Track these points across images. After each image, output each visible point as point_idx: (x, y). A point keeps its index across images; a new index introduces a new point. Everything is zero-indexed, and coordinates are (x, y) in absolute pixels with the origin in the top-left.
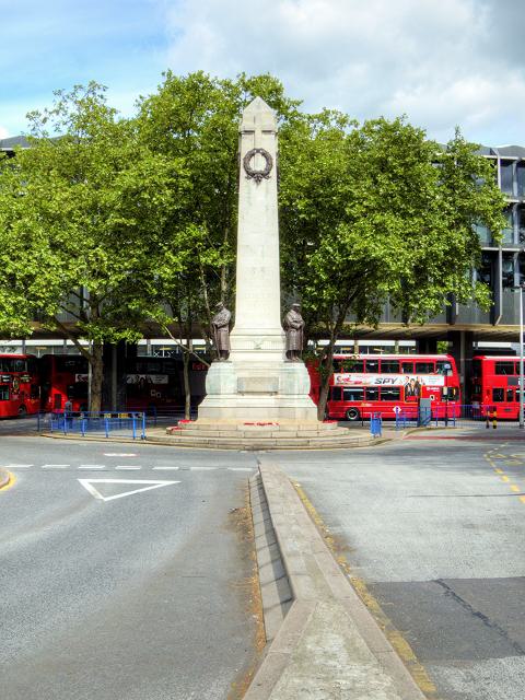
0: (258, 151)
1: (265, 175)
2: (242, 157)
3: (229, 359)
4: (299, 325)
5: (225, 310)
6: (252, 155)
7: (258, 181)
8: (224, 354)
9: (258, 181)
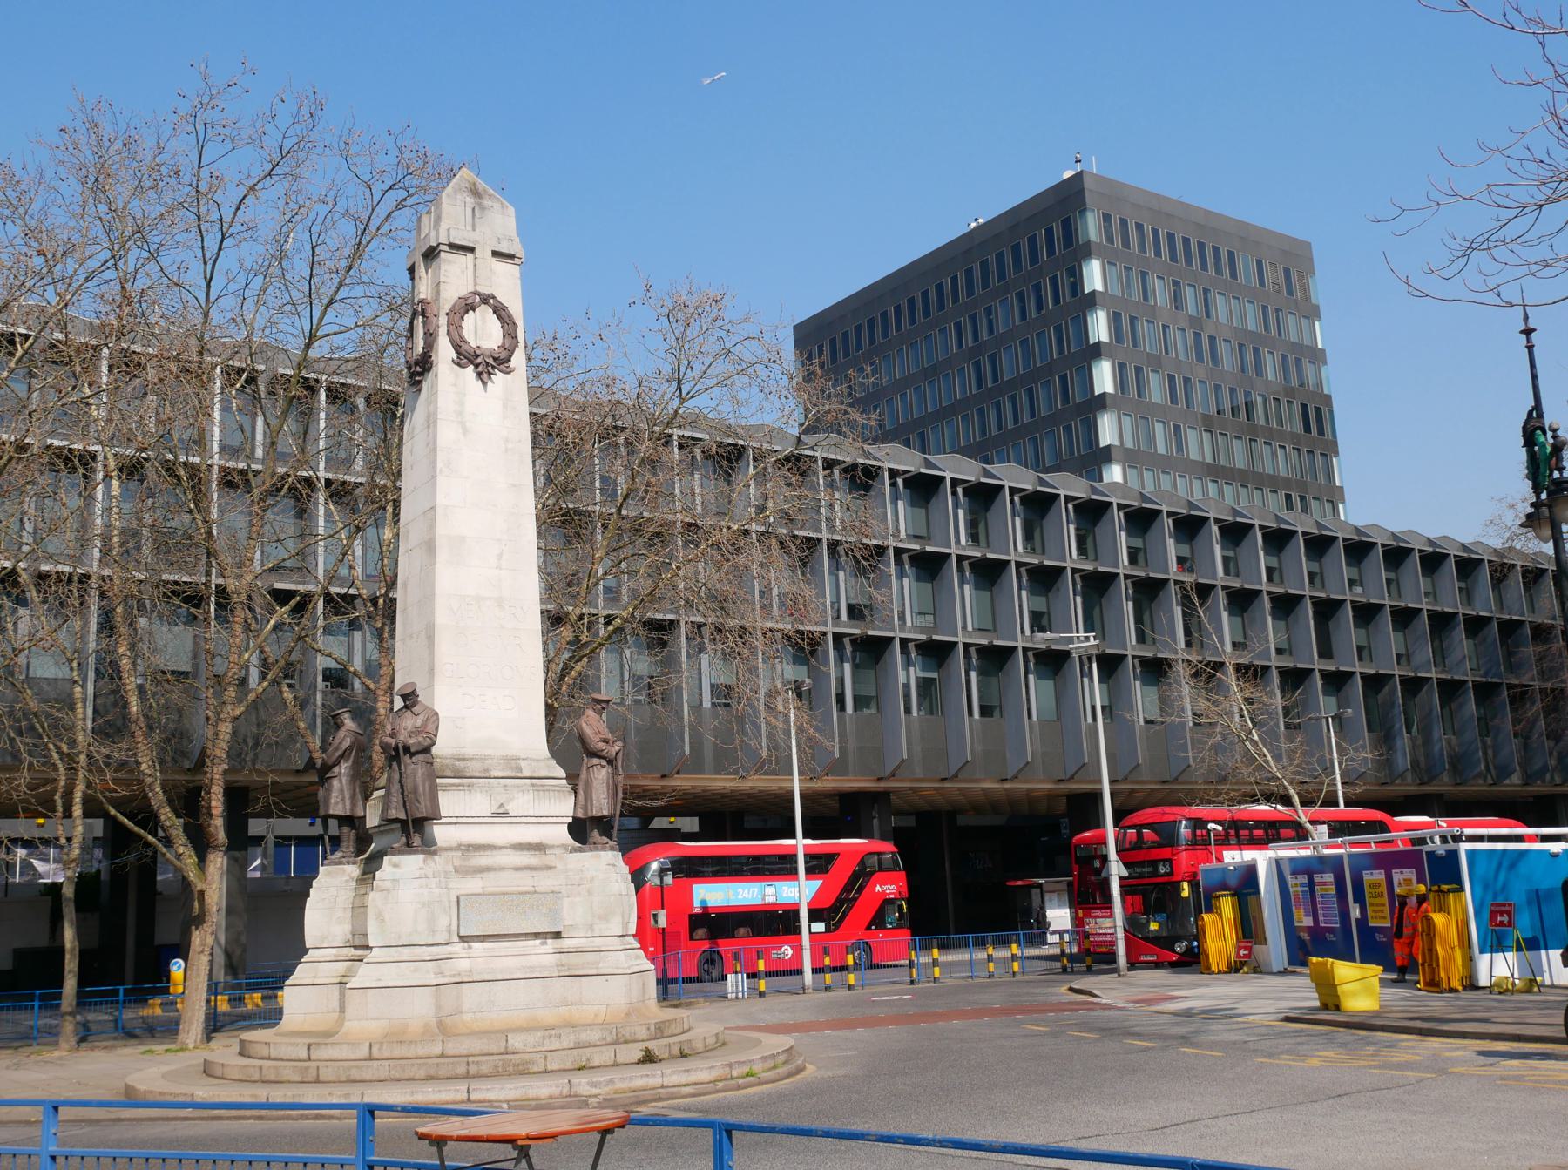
0: (485, 299)
1: (501, 361)
7: (483, 375)
9: (483, 375)
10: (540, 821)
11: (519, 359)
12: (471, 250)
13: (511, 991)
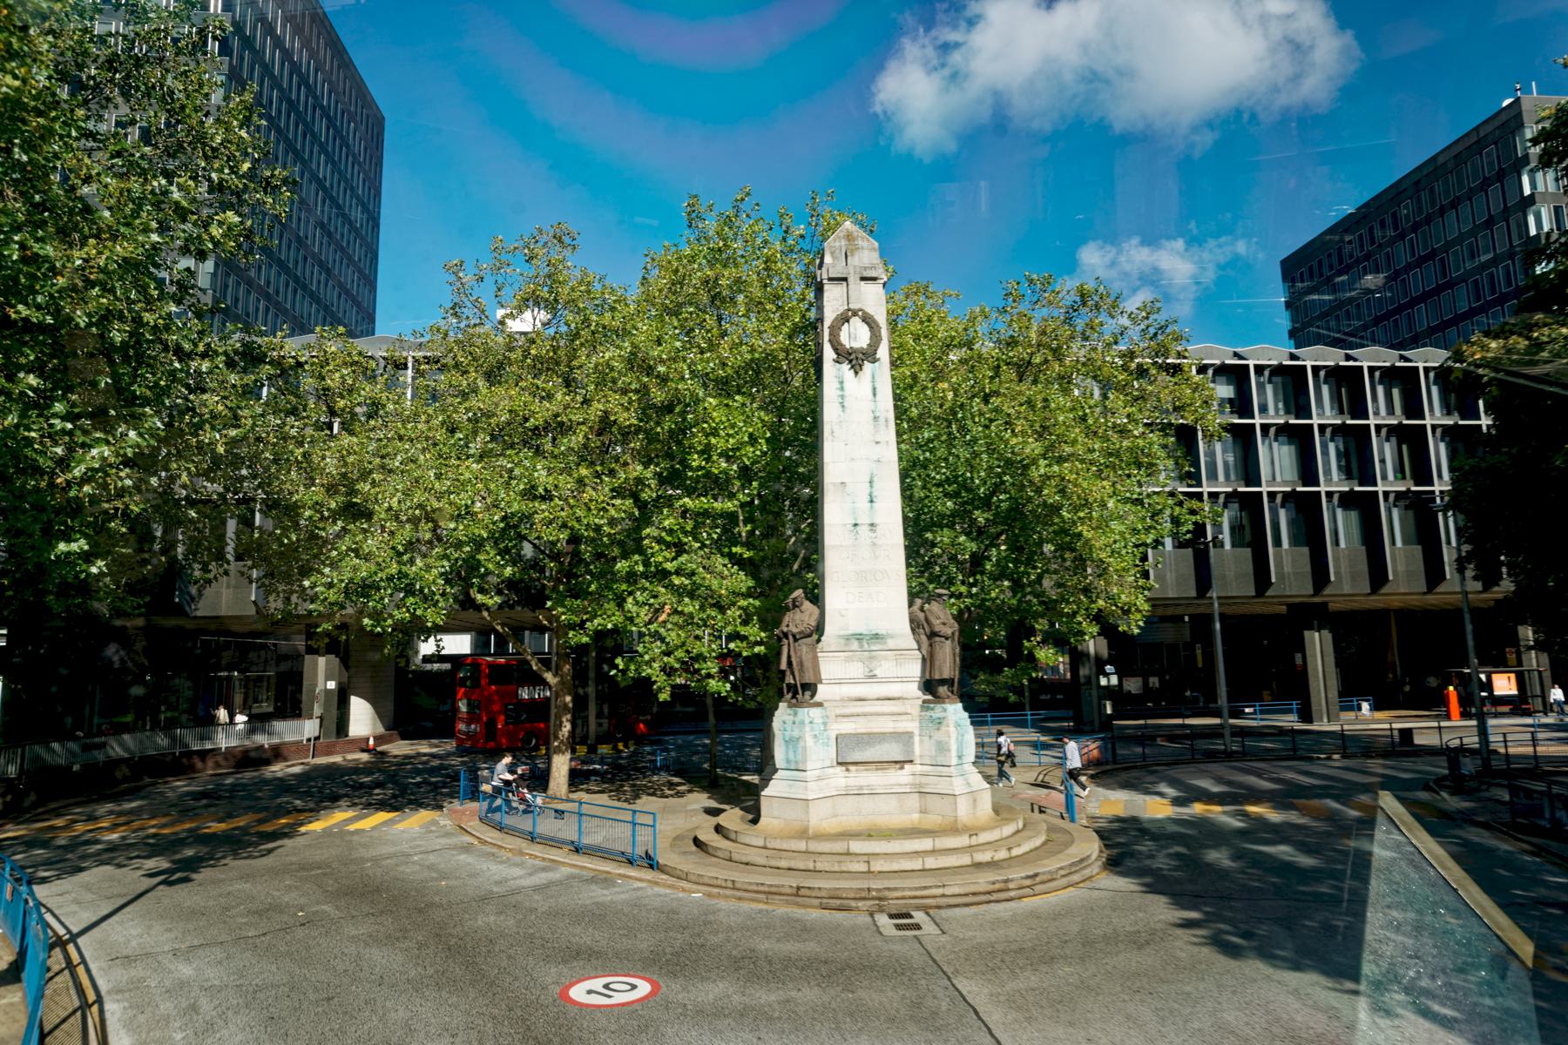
1: (870, 355)
2: (827, 323)
3: (817, 698)
4: (949, 632)
5: (807, 605)
6: (844, 318)
7: (857, 368)
8: (803, 691)
9: (857, 368)
10: (902, 680)
11: (883, 352)
12: (845, 279)
13: (885, 798)
